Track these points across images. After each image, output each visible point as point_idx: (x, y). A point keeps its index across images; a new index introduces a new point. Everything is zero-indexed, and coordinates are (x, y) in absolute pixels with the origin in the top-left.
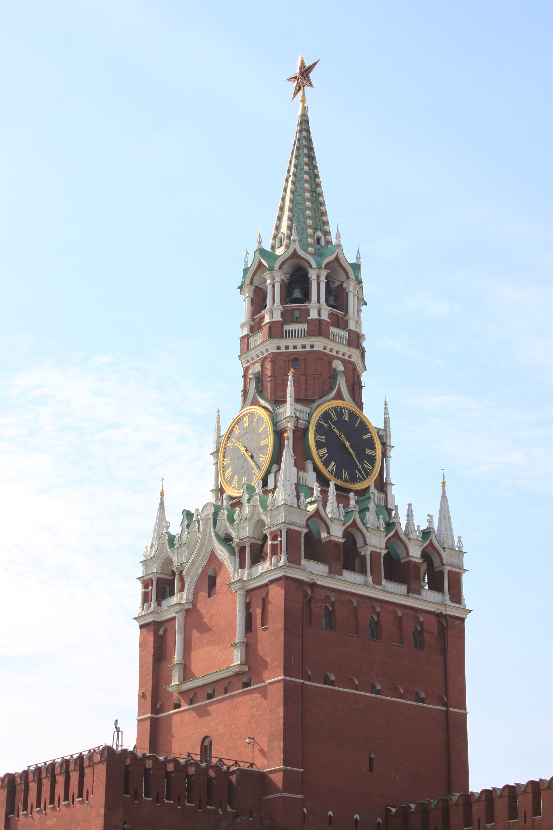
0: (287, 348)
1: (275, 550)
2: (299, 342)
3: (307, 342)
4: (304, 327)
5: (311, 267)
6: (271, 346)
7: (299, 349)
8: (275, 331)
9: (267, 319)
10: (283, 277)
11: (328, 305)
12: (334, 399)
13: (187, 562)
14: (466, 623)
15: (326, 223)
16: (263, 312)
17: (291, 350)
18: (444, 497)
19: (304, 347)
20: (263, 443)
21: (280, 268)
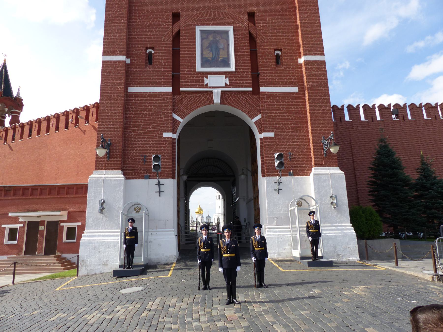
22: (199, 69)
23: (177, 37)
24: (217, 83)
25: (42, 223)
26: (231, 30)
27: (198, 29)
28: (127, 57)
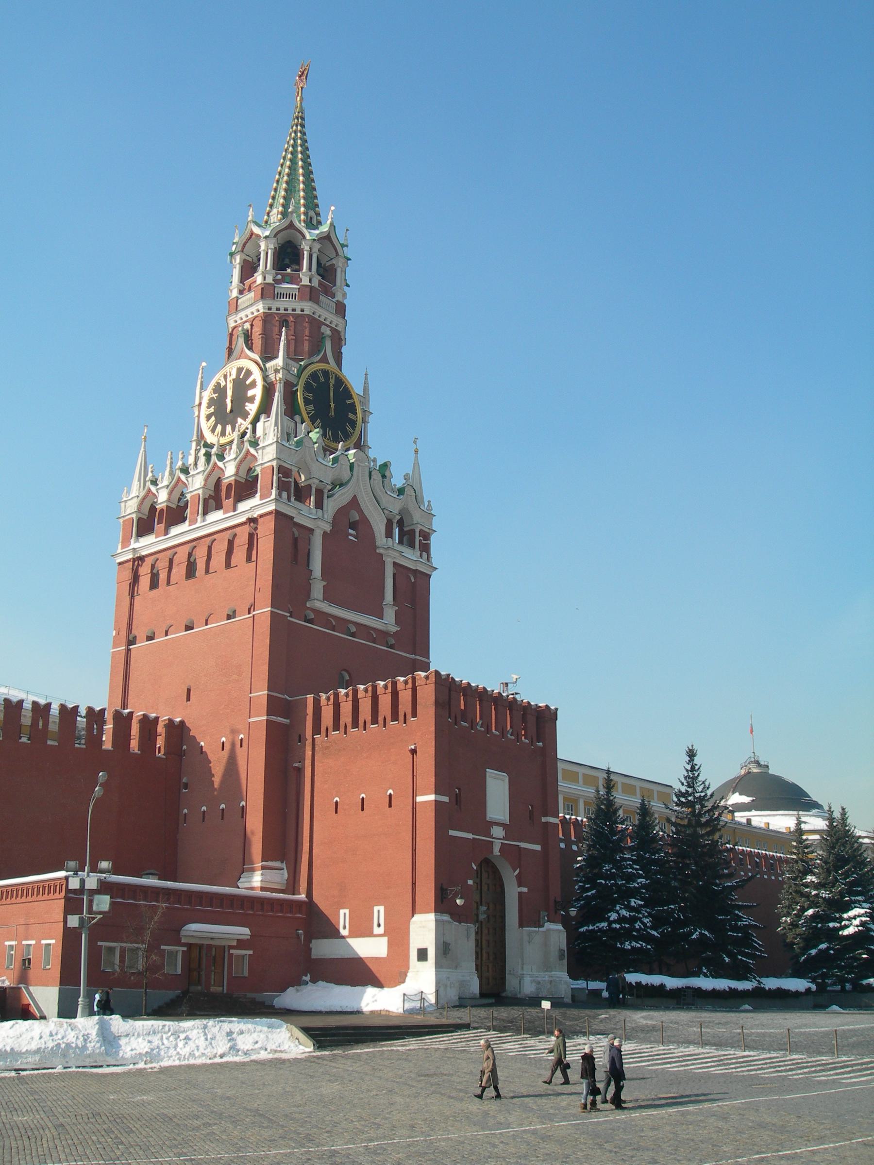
0: (278, 309)
5: (304, 237)
7: (290, 312)
8: (267, 292)
10: (276, 246)
11: (319, 275)
12: (319, 361)
14: (432, 580)
15: (317, 206)
16: (255, 275)
17: (282, 311)
18: (416, 465)
19: (294, 310)
20: (250, 393)
21: (275, 236)
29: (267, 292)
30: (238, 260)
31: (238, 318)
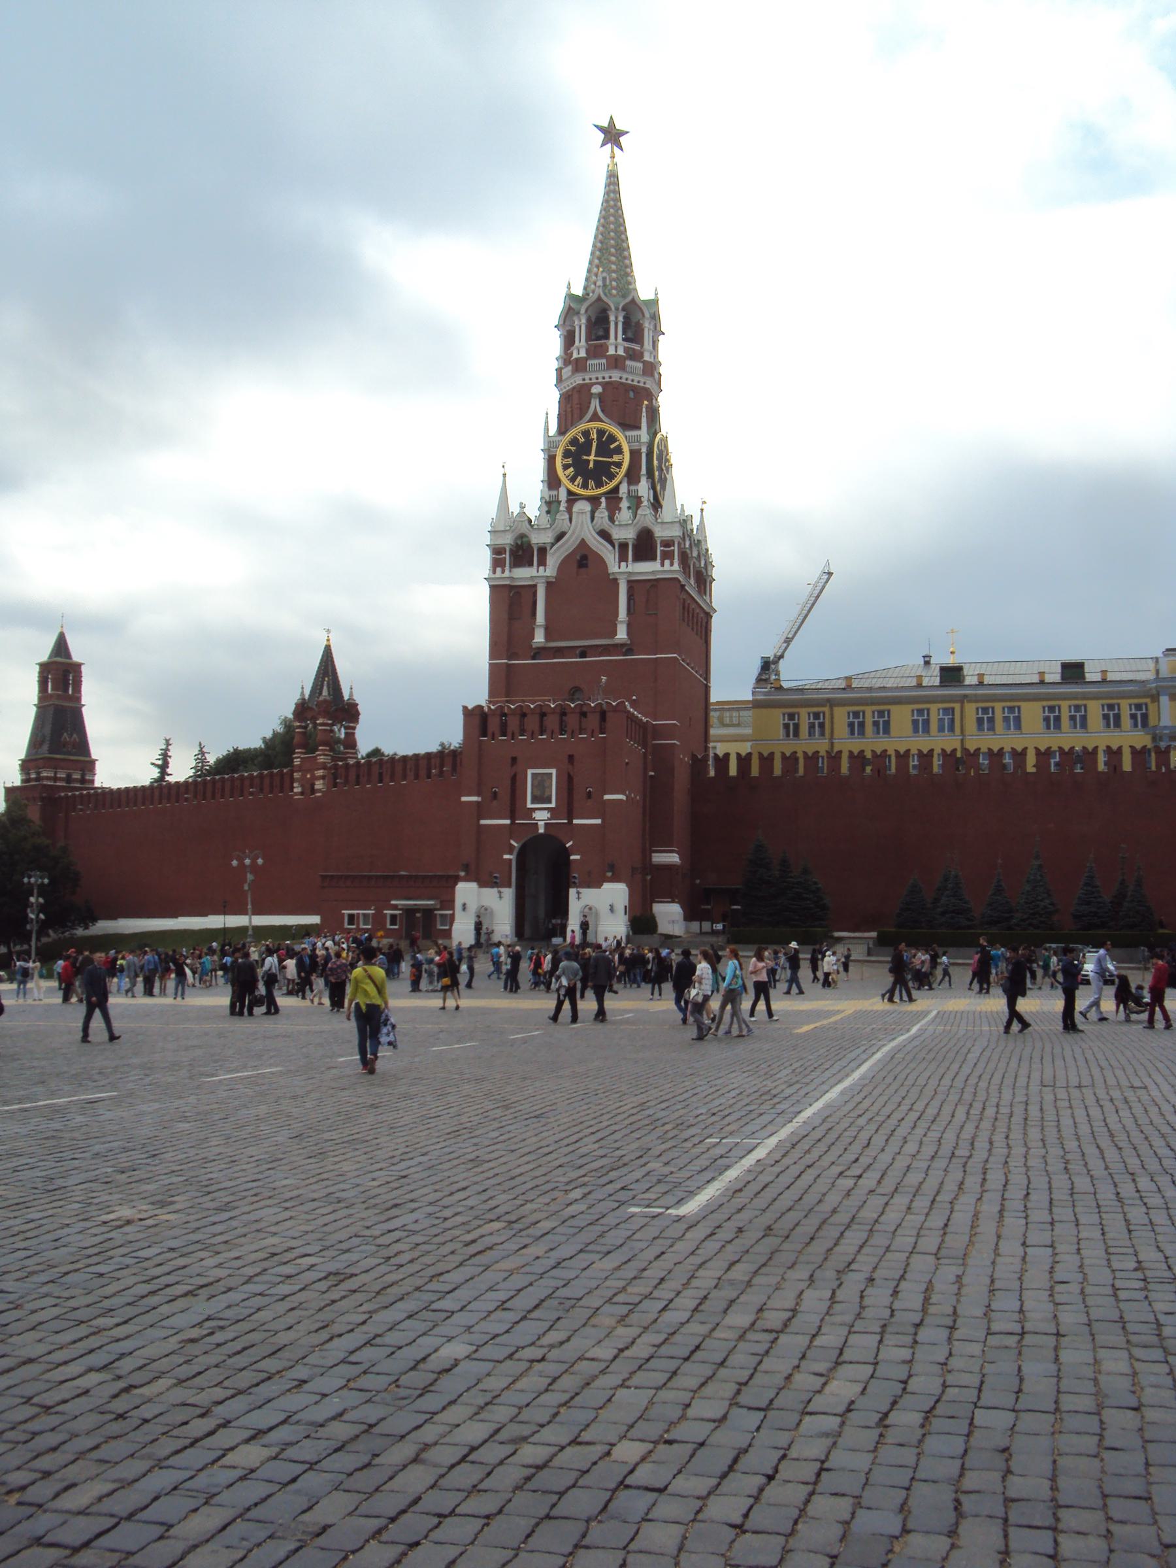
1: (667, 555)
2: (636, 379)
3: (642, 380)
4: (640, 365)
6: (616, 376)
9: (611, 352)
13: (553, 545)
14: (713, 620)
22: (529, 805)
23: (514, 779)
24: (542, 817)
25: (418, 910)
26: (554, 771)
27: (530, 772)
28: (478, 795)
29: (616, 363)
30: (584, 321)
31: (587, 377)
